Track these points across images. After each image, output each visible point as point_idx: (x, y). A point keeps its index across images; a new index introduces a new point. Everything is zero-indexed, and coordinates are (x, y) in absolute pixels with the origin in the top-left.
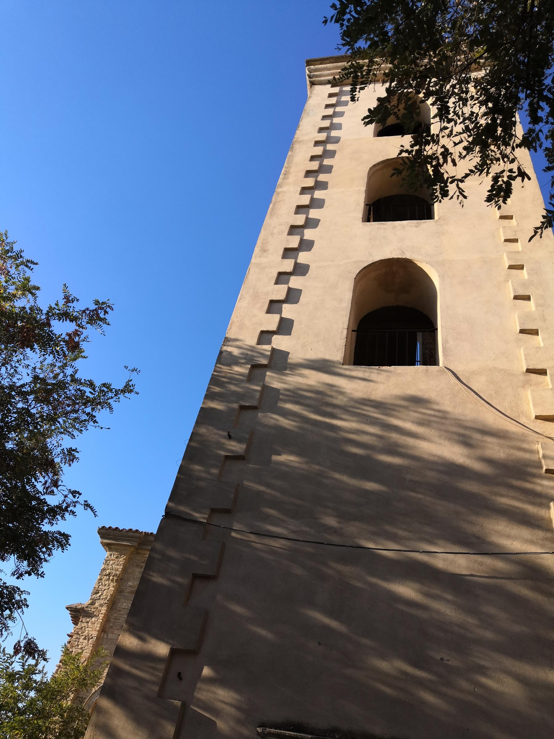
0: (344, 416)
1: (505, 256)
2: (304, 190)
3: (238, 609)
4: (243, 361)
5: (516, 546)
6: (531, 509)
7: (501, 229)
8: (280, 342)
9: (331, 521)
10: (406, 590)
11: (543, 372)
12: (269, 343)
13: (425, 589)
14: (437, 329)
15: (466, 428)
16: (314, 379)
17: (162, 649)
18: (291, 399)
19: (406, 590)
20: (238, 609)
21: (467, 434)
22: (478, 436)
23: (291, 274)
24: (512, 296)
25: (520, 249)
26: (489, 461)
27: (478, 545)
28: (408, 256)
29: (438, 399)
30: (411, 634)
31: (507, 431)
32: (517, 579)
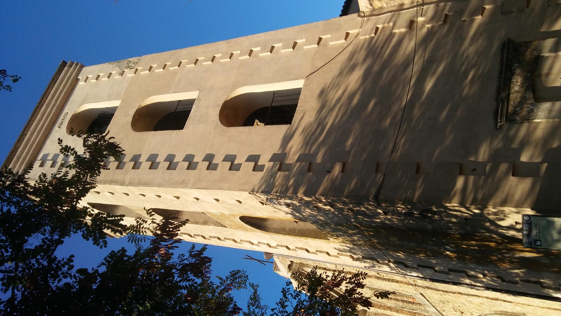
0: (326, 121)
1: (240, 58)
2: (136, 166)
3: (437, 152)
4: (272, 181)
5: (412, 44)
6: (395, 40)
7: (221, 61)
8: (264, 161)
9: (388, 121)
10: (429, 85)
11: (320, 39)
12: (264, 166)
13: (431, 74)
14: (274, 93)
15: (345, 67)
16: (296, 143)
17: (460, 182)
18: (309, 147)
19: (429, 85)
20: (437, 152)
21: (350, 67)
22: (353, 62)
23: (210, 163)
24: (269, 53)
25: (239, 52)
26: (364, 61)
27: (408, 62)
28: (221, 103)
29: (323, 85)
30: (453, 77)
31: (352, 51)
32: (426, 47)
